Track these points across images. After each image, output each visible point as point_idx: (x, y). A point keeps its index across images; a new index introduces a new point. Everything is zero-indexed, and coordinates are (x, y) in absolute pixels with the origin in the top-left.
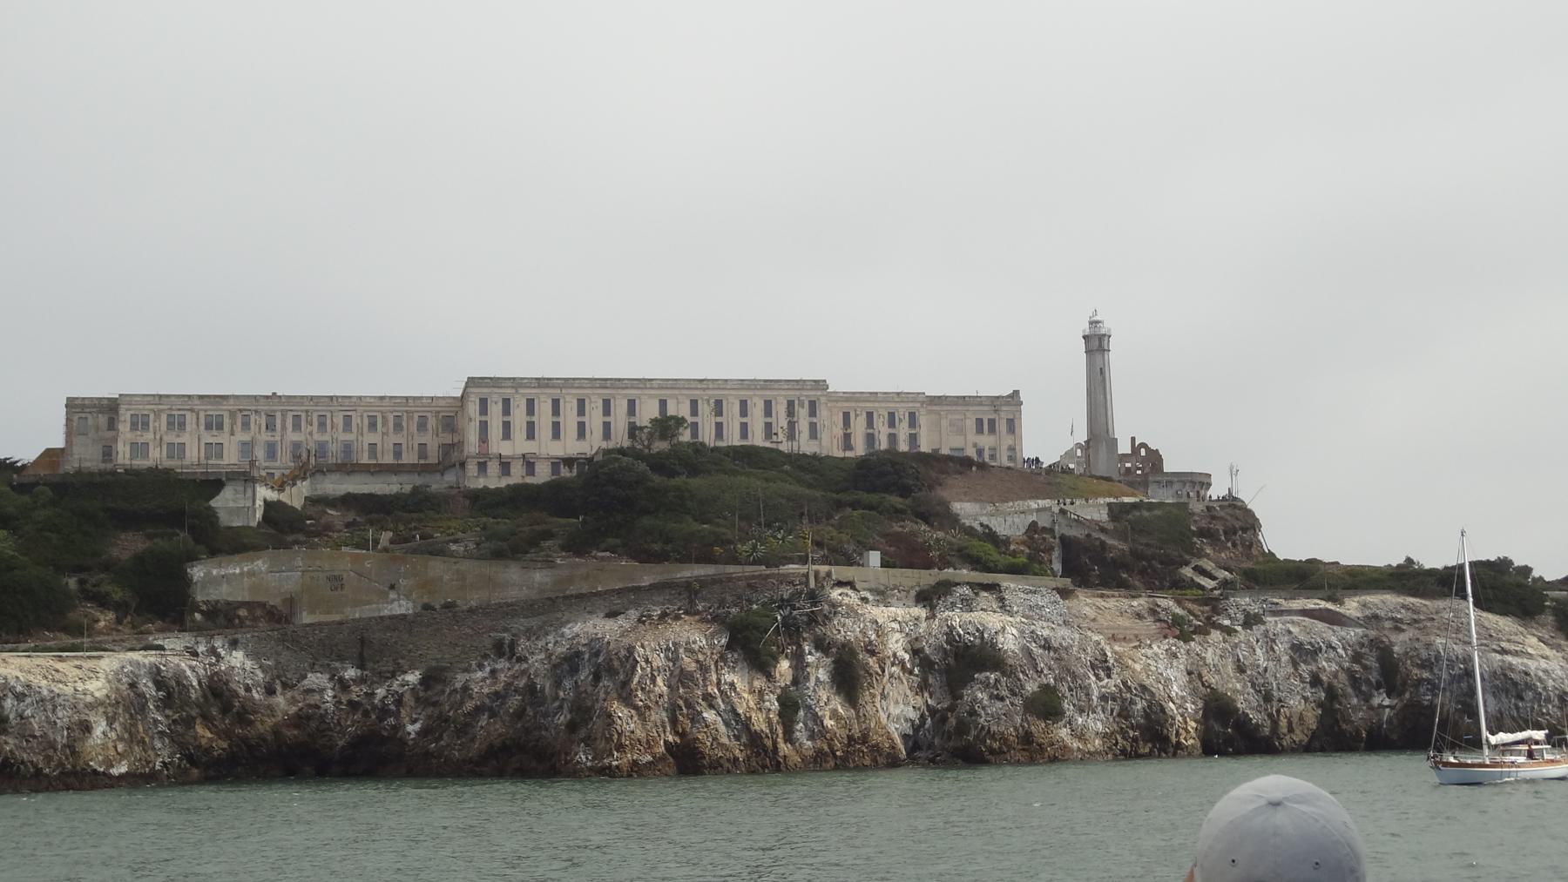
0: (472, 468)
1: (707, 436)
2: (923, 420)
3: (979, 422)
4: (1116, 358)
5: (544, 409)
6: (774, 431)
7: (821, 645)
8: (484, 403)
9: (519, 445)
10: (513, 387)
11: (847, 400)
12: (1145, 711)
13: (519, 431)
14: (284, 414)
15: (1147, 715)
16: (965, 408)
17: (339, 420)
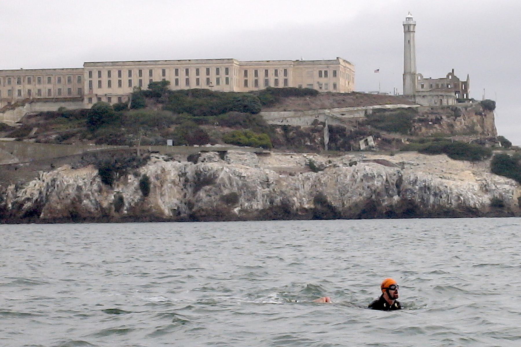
0: (86, 100)
1: (173, 87)
2: (290, 73)
3: (320, 72)
4: (418, 36)
5: (115, 74)
6: (210, 81)
7: (136, 175)
8: (90, 73)
9: (104, 91)
10: (102, 66)
11: (256, 65)
12: (281, 200)
13: (105, 84)
14: (24, 77)
15: (282, 202)
16: (314, 66)
17: (46, 79)
